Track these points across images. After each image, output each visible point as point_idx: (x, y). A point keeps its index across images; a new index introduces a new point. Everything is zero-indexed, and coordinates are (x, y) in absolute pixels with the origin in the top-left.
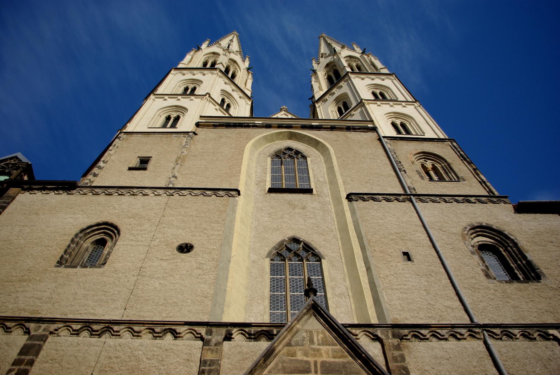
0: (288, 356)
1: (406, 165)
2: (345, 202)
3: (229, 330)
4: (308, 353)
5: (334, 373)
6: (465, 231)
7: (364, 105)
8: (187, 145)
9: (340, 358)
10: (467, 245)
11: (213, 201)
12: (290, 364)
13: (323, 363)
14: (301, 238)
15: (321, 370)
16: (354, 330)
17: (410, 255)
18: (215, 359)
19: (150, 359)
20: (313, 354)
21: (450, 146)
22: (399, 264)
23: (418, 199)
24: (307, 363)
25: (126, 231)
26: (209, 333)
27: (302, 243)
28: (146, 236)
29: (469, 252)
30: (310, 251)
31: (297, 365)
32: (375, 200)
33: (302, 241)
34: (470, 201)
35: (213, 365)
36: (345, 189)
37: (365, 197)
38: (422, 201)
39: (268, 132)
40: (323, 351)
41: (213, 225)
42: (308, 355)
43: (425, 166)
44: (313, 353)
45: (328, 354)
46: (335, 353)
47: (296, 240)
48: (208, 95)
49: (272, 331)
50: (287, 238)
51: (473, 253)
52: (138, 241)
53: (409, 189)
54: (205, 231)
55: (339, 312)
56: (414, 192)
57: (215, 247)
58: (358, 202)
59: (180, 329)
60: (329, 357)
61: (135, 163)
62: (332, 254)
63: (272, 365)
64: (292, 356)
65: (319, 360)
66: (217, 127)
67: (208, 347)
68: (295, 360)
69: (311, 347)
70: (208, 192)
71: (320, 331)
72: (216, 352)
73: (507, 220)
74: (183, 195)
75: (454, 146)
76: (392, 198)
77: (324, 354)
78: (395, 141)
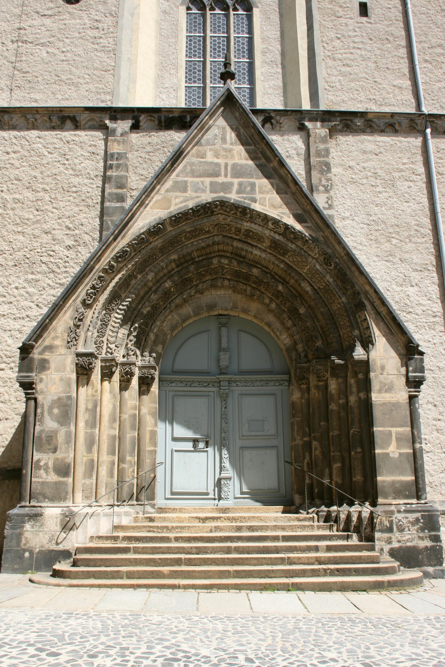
0: (197, 158)
4: (219, 154)
12: (200, 166)
18: (122, 151)
24: (217, 165)
31: (206, 167)
35: (121, 159)
44: (224, 153)
45: (240, 155)
60: (242, 159)
64: (202, 158)
65: (230, 162)
67: (113, 138)
68: (205, 162)
69: (223, 147)
72: (123, 143)
77: (236, 155)
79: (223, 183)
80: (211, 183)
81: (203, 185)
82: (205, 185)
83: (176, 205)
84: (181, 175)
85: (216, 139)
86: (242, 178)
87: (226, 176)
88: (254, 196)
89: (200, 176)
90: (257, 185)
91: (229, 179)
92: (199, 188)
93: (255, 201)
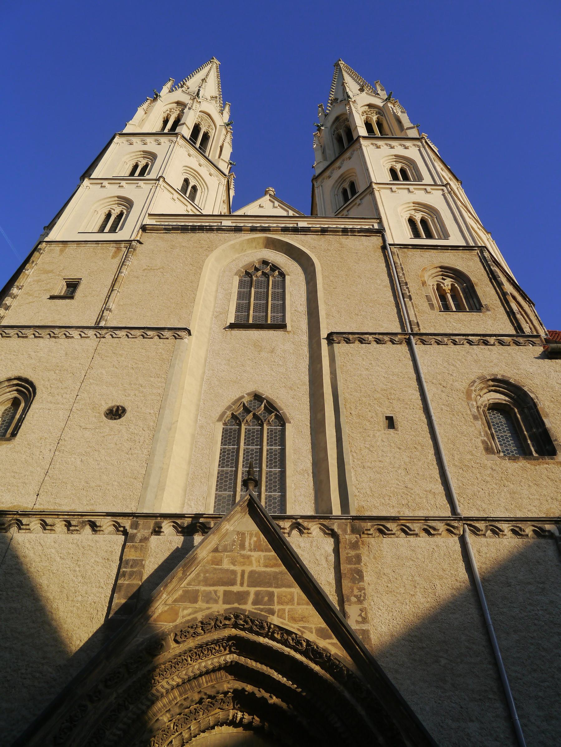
1: (414, 287)
2: (324, 343)
3: (159, 522)
4: (236, 561)
5: (262, 585)
6: (472, 386)
7: (372, 193)
8: (128, 260)
9: (272, 567)
10: (470, 406)
11: (154, 345)
12: (214, 574)
13: (252, 572)
14: (264, 395)
15: (248, 582)
16: (306, 523)
17: (395, 421)
18: (138, 558)
19: (64, 559)
20: (241, 562)
21: (479, 256)
22: (378, 434)
23: (419, 341)
24: (234, 572)
25: (44, 389)
26: (135, 526)
27: (265, 401)
28: (68, 396)
29: (471, 417)
30: (273, 412)
31: (221, 576)
32: (363, 341)
33: (264, 399)
34: (488, 342)
35: (136, 566)
36: (328, 324)
37: (351, 337)
38: (423, 342)
39: (236, 238)
40: (253, 559)
41: (152, 379)
42: (236, 563)
43: (442, 287)
45: (259, 562)
46: (267, 561)
47: (258, 397)
48: (161, 180)
49: (209, 523)
50: (246, 394)
51: (475, 418)
52: (58, 403)
53: (411, 325)
54: (141, 389)
55: (298, 494)
56: (416, 330)
57: (152, 412)
58: (340, 345)
59: (99, 521)
60: (260, 566)
61: (60, 288)
62: (300, 417)
63: (193, 575)
64: (217, 565)
65: (248, 569)
66: (170, 230)
67: (131, 544)
68: (220, 569)
69: (240, 554)
70: (150, 333)
71: (254, 533)
72: (141, 550)
73: (531, 370)
74: (118, 338)
75: (484, 258)
76: (386, 338)
77: (254, 562)
78: (406, 250)
79: (238, 593)
80: (225, 593)
81: (216, 595)
82: (218, 594)
83: (183, 617)
84: (193, 583)
85: (235, 545)
86: (260, 586)
87: (242, 584)
88: (272, 607)
89: (213, 585)
90: (276, 594)
91: (245, 588)
92: (211, 599)
93: (273, 614)
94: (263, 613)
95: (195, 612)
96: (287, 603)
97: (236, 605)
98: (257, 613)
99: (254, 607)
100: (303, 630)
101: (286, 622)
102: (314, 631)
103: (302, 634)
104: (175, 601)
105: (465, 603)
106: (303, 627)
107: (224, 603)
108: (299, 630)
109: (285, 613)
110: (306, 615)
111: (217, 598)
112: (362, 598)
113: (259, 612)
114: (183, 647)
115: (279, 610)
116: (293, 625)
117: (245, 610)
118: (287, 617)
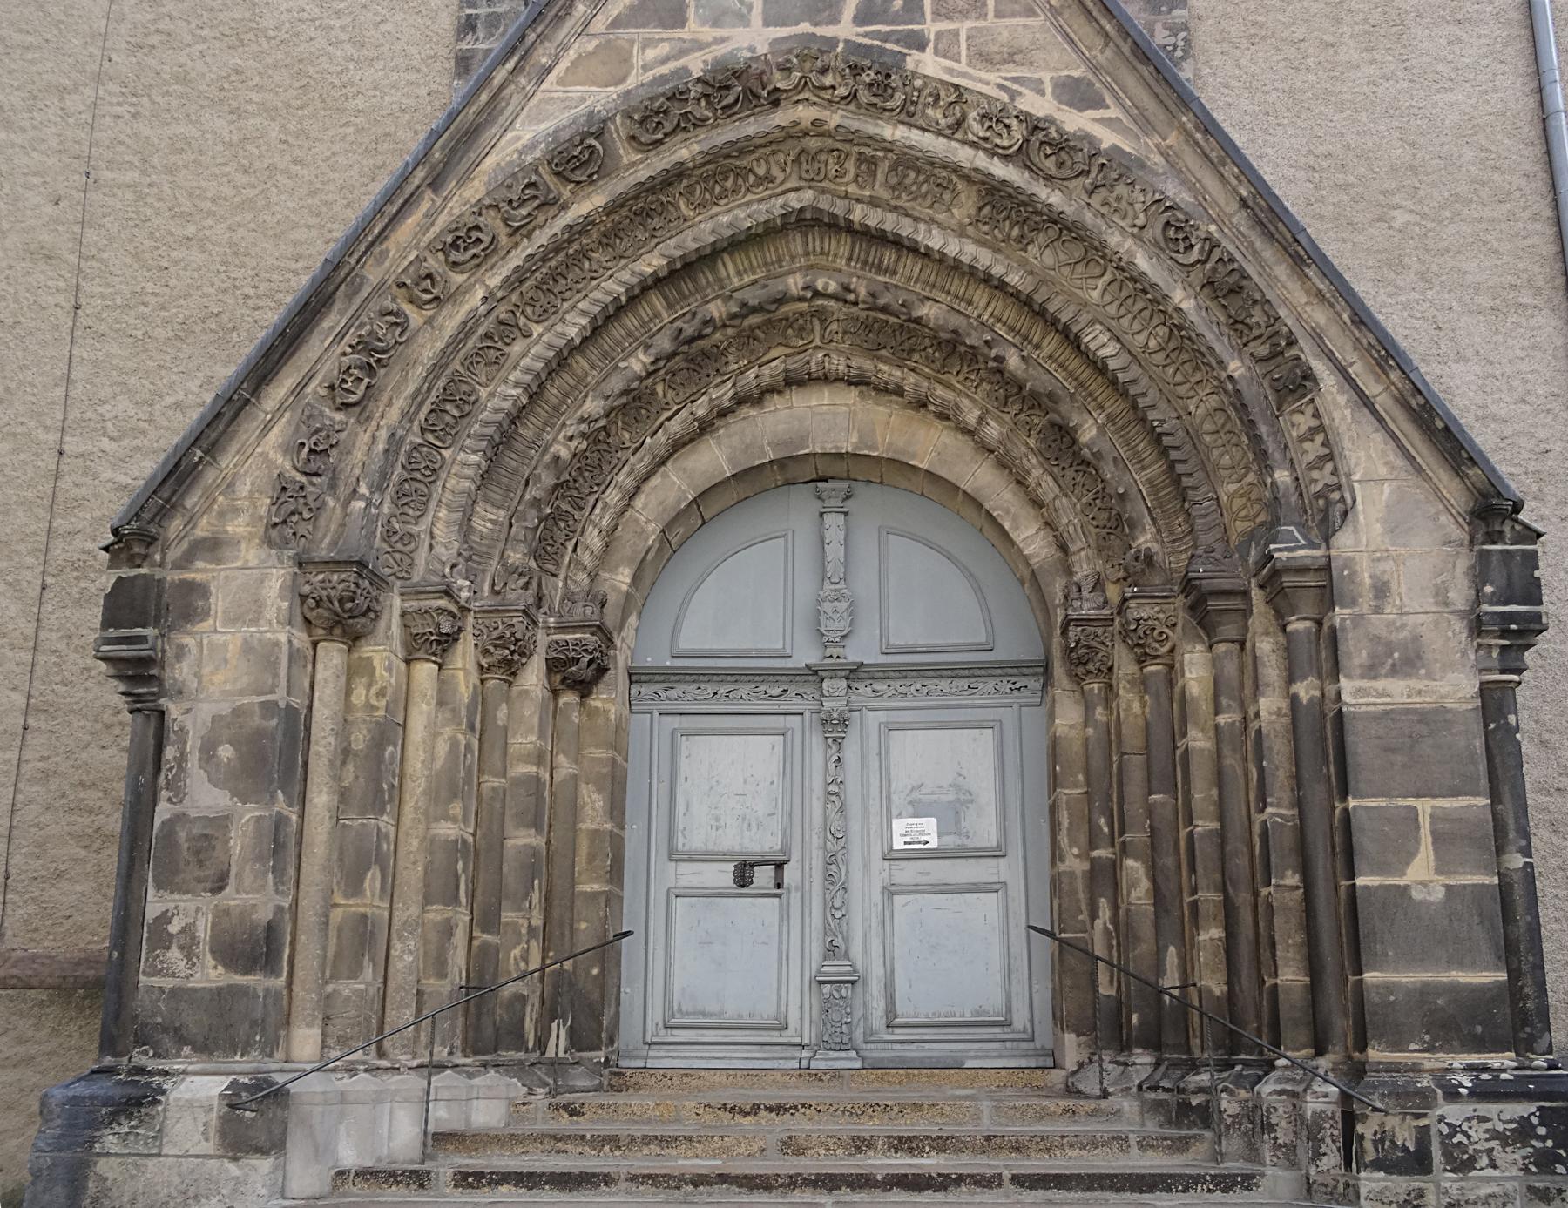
83: (646, 68)
94: (888, 46)
95: (682, 53)
96: (965, 15)
97: (805, 27)
98: (872, 46)
99: (861, 30)
100: (1015, 87)
101: (963, 66)
102: (1049, 89)
103: (1012, 99)
104: (616, 23)
105: (1486, 62)
106: (1015, 80)
107: (767, 23)
108: (1001, 87)
109: (958, 44)
110: (1025, 44)
111: (744, 10)
112: (1179, 53)
113: (877, 43)
114: (660, 162)
115: (939, 35)
116: (983, 75)
117: (832, 42)
118: (964, 52)
